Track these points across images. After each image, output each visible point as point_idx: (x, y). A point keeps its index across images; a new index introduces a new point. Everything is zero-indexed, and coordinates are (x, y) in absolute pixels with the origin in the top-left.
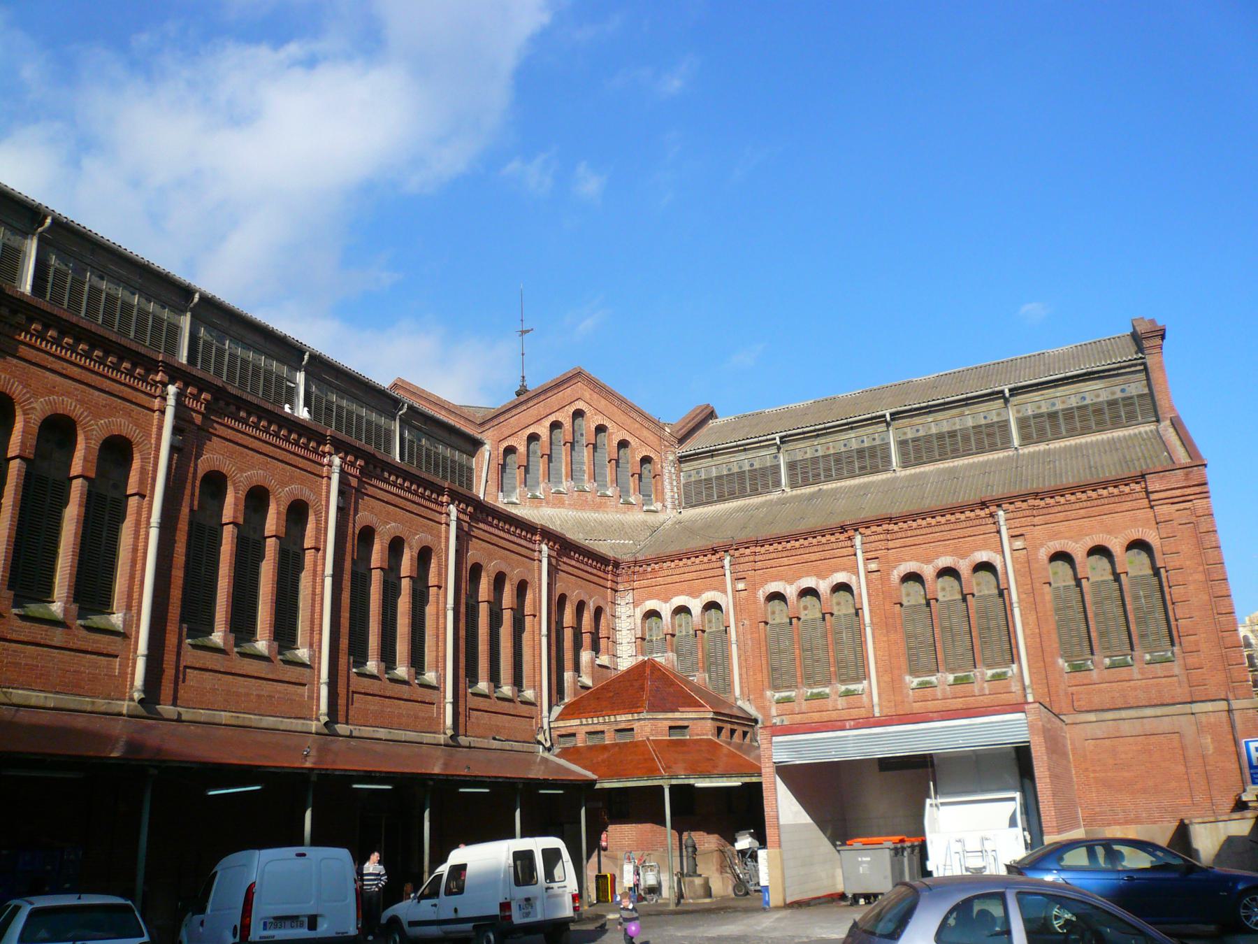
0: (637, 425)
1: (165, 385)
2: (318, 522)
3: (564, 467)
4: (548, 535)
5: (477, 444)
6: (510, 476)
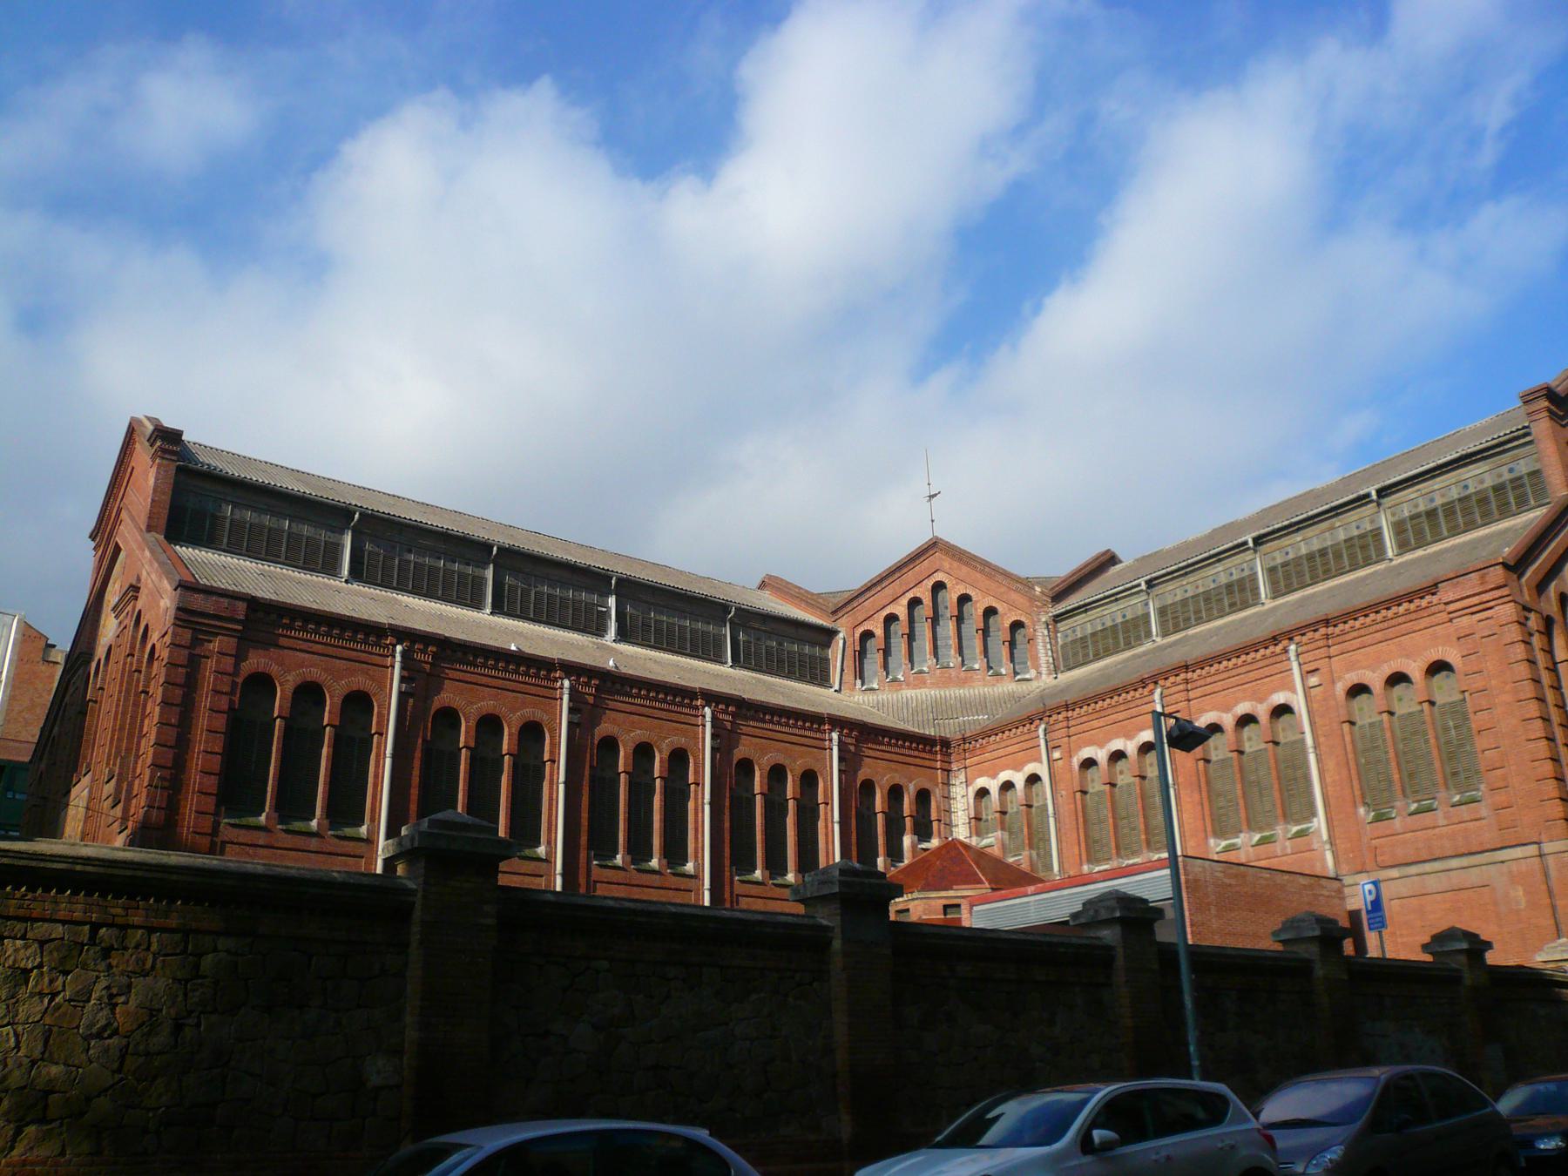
0: (1003, 589)
1: (394, 646)
2: (552, 738)
3: (927, 644)
4: (838, 722)
5: (832, 633)
6: (870, 661)
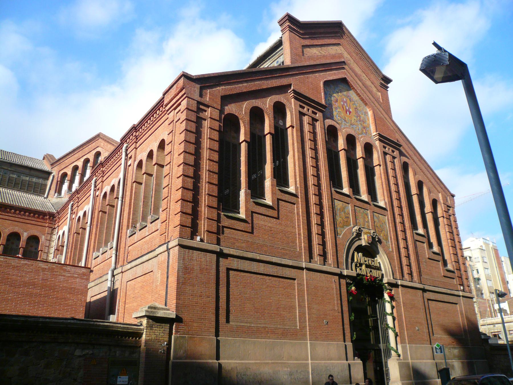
5: (49, 173)
